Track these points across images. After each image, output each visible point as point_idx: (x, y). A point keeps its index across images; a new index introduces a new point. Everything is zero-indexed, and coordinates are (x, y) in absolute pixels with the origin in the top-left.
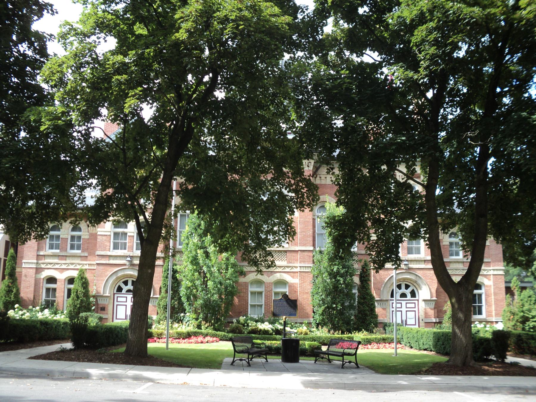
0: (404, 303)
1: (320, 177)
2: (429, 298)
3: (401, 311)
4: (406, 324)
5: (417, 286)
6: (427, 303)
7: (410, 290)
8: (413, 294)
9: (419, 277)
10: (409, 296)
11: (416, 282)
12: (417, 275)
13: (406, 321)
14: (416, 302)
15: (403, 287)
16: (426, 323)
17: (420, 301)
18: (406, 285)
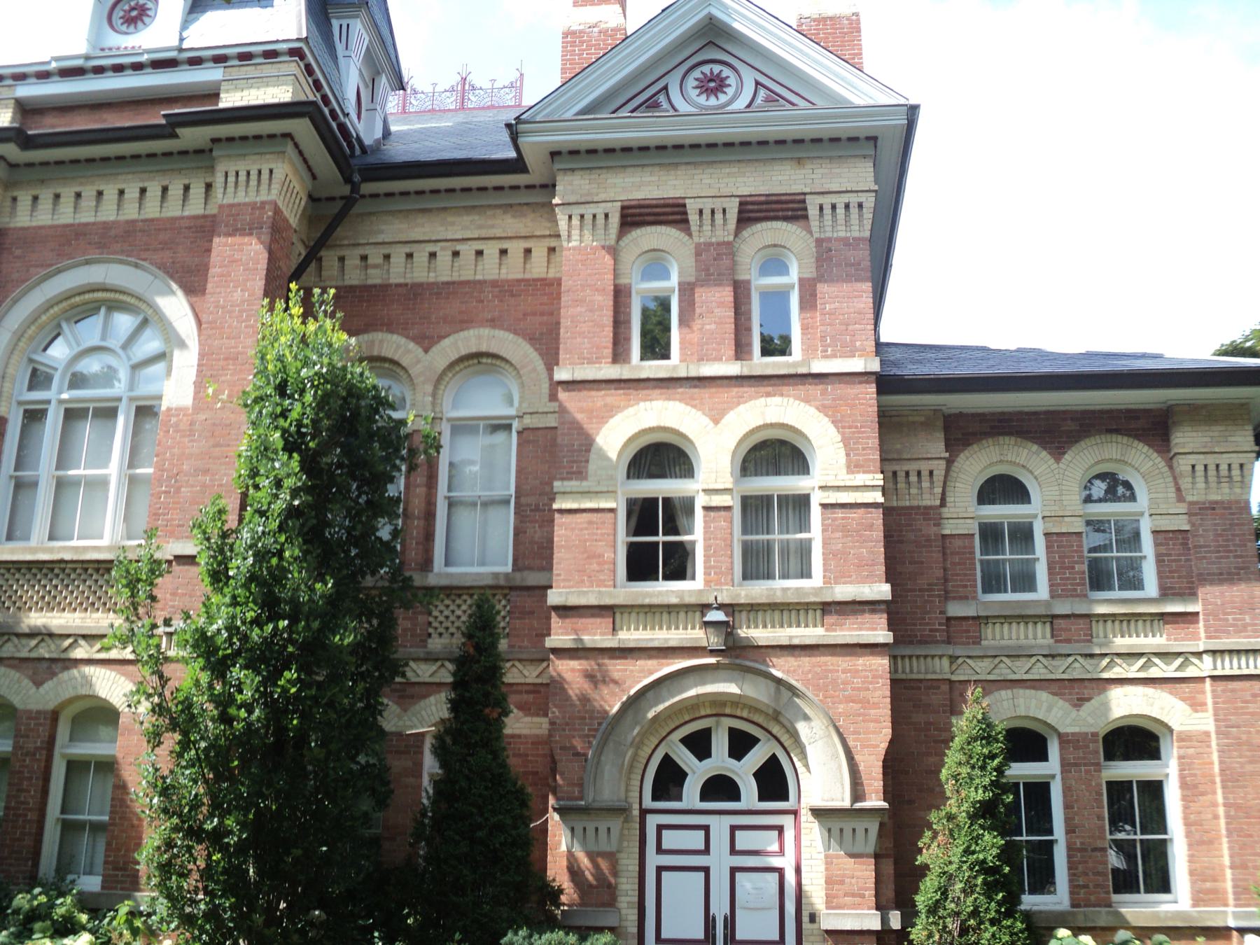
0: (720, 827)
1: (364, 258)
2: (846, 804)
3: (706, 870)
5: (785, 738)
6: (836, 825)
7: (756, 758)
8: (773, 782)
9: (791, 688)
12: (779, 681)
13: (730, 922)
14: (787, 821)
15: (720, 744)
17: (806, 816)
18: (735, 735)
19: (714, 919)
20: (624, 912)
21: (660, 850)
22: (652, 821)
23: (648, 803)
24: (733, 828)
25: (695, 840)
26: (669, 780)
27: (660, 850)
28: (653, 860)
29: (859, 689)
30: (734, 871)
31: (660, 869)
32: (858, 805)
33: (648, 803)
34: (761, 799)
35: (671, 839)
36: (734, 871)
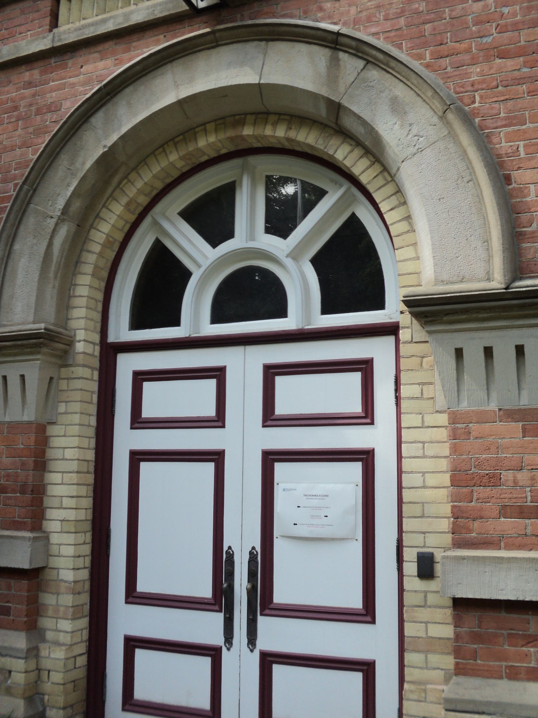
0: (244, 368)
2: (497, 283)
3: (217, 458)
4: (263, 601)
5: (360, 168)
6: (473, 342)
7: (315, 226)
8: (351, 271)
9: (360, 49)
10: (302, 285)
11: (334, 119)
12: (333, 42)
14: (380, 351)
16: (460, 604)
19: (230, 557)
20: (54, 539)
21: (138, 421)
22: (127, 365)
23: (121, 330)
24: (271, 372)
25: (199, 398)
26: (161, 289)
27: (138, 421)
28: (126, 439)
29: (516, 27)
30: (270, 459)
31: (137, 458)
32: (526, 284)
33: (121, 330)
34: (326, 310)
35: (159, 400)
36: (270, 459)
